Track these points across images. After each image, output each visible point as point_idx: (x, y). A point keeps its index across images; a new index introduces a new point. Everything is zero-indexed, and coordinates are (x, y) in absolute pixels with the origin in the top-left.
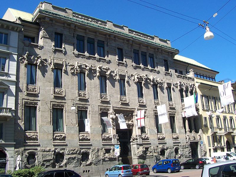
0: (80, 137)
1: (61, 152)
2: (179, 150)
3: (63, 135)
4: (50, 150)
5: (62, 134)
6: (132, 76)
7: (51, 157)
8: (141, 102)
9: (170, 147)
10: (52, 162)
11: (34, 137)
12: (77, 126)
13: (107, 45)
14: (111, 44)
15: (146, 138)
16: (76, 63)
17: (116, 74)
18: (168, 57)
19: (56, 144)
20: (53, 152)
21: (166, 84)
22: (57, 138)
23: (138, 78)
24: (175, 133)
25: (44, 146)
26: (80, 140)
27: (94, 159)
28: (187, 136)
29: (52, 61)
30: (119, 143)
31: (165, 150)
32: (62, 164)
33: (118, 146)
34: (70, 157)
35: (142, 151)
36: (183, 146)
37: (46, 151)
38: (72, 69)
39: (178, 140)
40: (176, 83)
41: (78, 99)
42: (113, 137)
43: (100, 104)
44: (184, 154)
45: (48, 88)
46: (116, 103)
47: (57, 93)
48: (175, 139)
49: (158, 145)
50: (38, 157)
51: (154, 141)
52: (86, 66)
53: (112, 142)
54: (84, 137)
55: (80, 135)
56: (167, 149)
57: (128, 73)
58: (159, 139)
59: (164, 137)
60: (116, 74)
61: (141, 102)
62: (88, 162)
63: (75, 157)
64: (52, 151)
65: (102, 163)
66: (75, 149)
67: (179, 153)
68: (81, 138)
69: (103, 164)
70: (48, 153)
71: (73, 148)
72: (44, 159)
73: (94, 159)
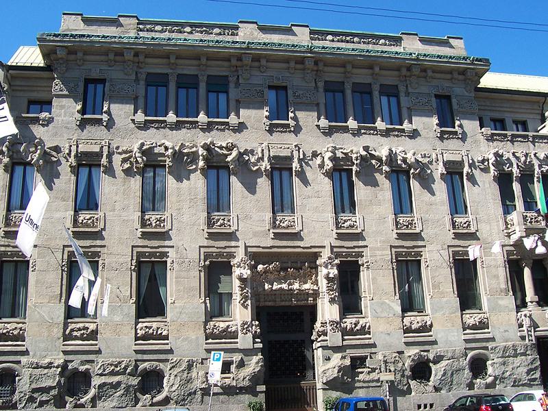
0: (139, 331)
1: (82, 368)
2: (489, 363)
3: (92, 327)
4: (51, 363)
5: (87, 325)
6: (315, 155)
7: (51, 379)
8: (346, 224)
9: (450, 355)
10: (54, 392)
11: (15, 332)
12: (131, 301)
13: (237, 84)
14: (248, 79)
15: (358, 328)
16: (134, 142)
17: (260, 155)
18: (451, 85)
19: (70, 348)
20: (59, 369)
21: (441, 164)
22: (75, 333)
23: (331, 159)
24: (478, 311)
25: (38, 353)
26: (137, 339)
27: (174, 389)
28: (523, 317)
29: (74, 148)
30: (261, 346)
31: (431, 364)
32: (82, 401)
33: (220, 354)
34: (103, 381)
35: (337, 368)
36: (505, 349)
37: (41, 367)
38: (124, 161)
39: (486, 330)
40: (480, 159)
41: (139, 234)
42: (240, 329)
43: (206, 243)
44: (508, 373)
45: (58, 215)
46: (255, 234)
48: (474, 327)
49: (402, 347)
50: (19, 380)
51: (387, 337)
52: (167, 149)
53: (237, 343)
54: (151, 331)
55: (140, 325)
56: (438, 359)
57: (301, 150)
58: (407, 330)
59: (429, 323)
61: (346, 224)
62: (159, 397)
63: (119, 383)
64: (57, 367)
65: (199, 400)
66: (120, 363)
67: (490, 370)
68: (140, 333)
69: (202, 401)
70: (46, 371)
71: (114, 360)
72: (34, 386)
73: (174, 389)
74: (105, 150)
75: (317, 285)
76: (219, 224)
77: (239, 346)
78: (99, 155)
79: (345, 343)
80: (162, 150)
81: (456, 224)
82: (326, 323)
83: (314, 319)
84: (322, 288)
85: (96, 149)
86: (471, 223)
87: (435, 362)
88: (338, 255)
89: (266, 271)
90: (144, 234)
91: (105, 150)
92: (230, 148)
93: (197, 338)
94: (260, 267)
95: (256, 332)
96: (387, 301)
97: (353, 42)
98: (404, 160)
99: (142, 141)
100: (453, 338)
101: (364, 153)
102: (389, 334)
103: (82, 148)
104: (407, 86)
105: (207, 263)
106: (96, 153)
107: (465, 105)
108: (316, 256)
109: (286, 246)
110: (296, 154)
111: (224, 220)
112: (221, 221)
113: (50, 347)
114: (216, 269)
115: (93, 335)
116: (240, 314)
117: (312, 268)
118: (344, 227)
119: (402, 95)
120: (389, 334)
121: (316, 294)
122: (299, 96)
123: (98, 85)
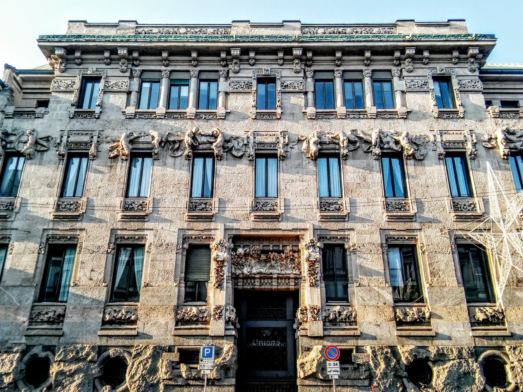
1: (43, 354)
8: (332, 207)
13: (227, 77)
14: (237, 73)
15: (343, 317)
18: (451, 65)
19: (33, 332)
20: (18, 355)
21: (439, 145)
27: (135, 379)
31: (430, 364)
43: (185, 226)
47: (65, 208)
48: (486, 322)
49: (394, 341)
52: (153, 138)
55: (109, 310)
56: (441, 358)
60: (246, 142)
74: (95, 139)
75: (299, 269)
76: (200, 207)
77: (210, 333)
78: (88, 144)
79: (326, 333)
80: (148, 139)
81: (459, 206)
82: (306, 310)
83: (296, 305)
84: (304, 272)
85: (86, 139)
86: (477, 205)
87: (434, 362)
88: (320, 238)
89: (246, 255)
90: (124, 217)
91: (95, 139)
92: (214, 136)
93: (167, 324)
94: (241, 251)
95: (229, 318)
96: (376, 288)
97: (345, 33)
98: (397, 142)
99: (131, 131)
100: (458, 334)
101: (353, 138)
102: (379, 326)
103: (72, 139)
104: (401, 71)
105: (186, 246)
106: (86, 143)
107: (468, 84)
108: (297, 238)
109: (265, 228)
110: (281, 140)
111: (206, 204)
112: (203, 206)
113: (13, 332)
114: (194, 251)
115: (60, 318)
116: (218, 297)
117: (294, 252)
118: (329, 210)
119: (396, 80)
120: (379, 326)
121: (298, 279)
122: (286, 86)
123: (96, 85)
